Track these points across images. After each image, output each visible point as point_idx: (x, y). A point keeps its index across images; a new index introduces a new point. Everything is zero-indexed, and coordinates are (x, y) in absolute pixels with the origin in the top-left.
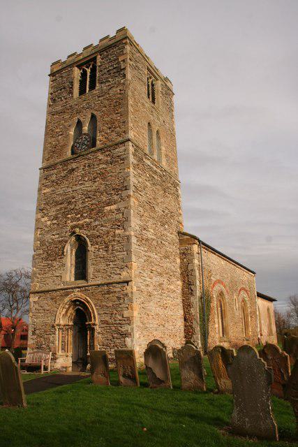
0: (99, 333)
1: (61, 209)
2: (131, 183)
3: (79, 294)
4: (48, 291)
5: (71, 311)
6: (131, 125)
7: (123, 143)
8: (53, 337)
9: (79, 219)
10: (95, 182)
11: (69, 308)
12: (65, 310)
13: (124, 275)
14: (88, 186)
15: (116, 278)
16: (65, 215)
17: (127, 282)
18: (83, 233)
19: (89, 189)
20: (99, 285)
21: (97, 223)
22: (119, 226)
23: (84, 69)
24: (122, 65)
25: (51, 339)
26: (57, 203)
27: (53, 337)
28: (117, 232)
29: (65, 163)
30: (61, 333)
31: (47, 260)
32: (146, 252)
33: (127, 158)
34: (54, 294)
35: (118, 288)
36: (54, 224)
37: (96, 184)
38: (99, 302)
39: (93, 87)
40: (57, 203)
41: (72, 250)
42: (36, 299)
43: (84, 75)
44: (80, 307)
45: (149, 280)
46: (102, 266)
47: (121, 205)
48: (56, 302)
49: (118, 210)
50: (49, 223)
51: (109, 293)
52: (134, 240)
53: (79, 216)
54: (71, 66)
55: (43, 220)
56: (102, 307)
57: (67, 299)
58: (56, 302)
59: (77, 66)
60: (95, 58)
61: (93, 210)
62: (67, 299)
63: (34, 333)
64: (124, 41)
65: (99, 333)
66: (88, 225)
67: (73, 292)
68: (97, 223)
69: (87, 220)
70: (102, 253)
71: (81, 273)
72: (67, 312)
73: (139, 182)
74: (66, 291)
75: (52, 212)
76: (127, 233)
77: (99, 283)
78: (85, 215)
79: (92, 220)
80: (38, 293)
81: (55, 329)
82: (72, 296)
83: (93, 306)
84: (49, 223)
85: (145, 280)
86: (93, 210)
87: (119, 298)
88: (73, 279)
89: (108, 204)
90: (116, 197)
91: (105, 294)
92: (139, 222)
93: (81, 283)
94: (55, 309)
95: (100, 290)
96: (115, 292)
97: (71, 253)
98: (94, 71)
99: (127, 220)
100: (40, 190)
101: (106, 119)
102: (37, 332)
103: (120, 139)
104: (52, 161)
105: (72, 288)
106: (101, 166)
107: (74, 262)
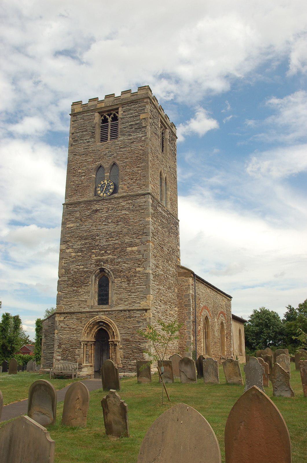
0: (121, 348)
1: (86, 244)
2: (151, 231)
3: (104, 317)
4: (74, 313)
5: (95, 330)
6: (150, 179)
7: (144, 195)
8: (79, 351)
9: (103, 255)
10: (118, 225)
11: (93, 327)
12: (89, 329)
13: (143, 304)
14: (111, 227)
15: (136, 306)
16: (91, 248)
17: (146, 310)
18: (107, 267)
19: (113, 230)
20: (121, 311)
21: (119, 260)
22: (139, 264)
23: (105, 117)
24: (143, 123)
25: (77, 352)
26: (81, 238)
27: (79, 351)
28: (138, 269)
29: (89, 203)
30: (85, 347)
31: (72, 286)
32: (158, 285)
33: (147, 209)
34: (80, 315)
35: (138, 314)
36: (78, 256)
37: (119, 227)
38: (121, 324)
39: (115, 135)
40: (81, 238)
41: (95, 280)
42: (62, 319)
43: (105, 121)
44: (103, 328)
45: (159, 307)
46: (124, 295)
47: (142, 248)
49: (139, 251)
50: (73, 254)
51: (130, 317)
52: (151, 277)
53: (103, 252)
54: (92, 111)
55: (68, 251)
56: (124, 328)
57: (91, 320)
59: (98, 112)
60: (118, 109)
61: (116, 249)
63: (59, 347)
64: (145, 101)
65: (121, 348)
66: (112, 261)
67: (97, 315)
68: (119, 260)
69: (110, 256)
70: (124, 285)
71: (103, 299)
72: (91, 330)
73: (155, 229)
74: (91, 314)
75: (78, 245)
76: (147, 271)
77: (121, 309)
78: (109, 252)
79: (116, 257)
80: (64, 313)
81: (81, 344)
82: (97, 318)
83: (116, 327)
84: (73, 254)
85: (157, 308)
86: (116, 249)
87: (138, 322)
88: (96, 304)
89: (131, 245)
90: (137, 241)
91: (127, 318)
92: (154, 262)
93: (104, 307)
94: (81, 328)
96: (136, 317)
97: (95, 282)
98: (115, 119)
99: (146, 260)
100: (64, 224)
101: (128, 170)
102: (63, 346)
103: (140, 192)
104: (75, 199)
105: (97, 312)
106: (124, 212)
107: (97, 290)
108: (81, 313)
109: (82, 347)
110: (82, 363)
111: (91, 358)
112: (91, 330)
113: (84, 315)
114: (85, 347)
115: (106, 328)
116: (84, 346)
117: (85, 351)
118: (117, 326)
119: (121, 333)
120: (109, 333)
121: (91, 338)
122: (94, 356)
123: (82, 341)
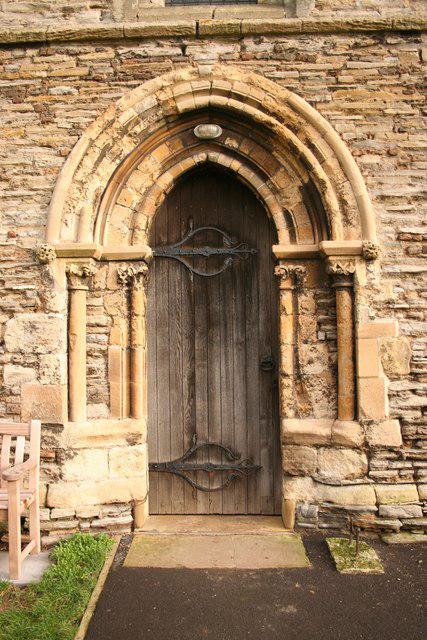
0: (389, 306)
5: (155, 176)
11: (141, 154)
12: (108, 167)
38: (384, 129)
44: (222, 159)
48: (46, 117)
57: (136, 102)
58: (46, 117)
62: (136, 102)
65: (389, 306)
67: (184, 58)
72: (119, 179)
82: (184, 87)
83: (346, 152)
94: (46, 157)
95: (388, 61)
108: (39, 43)
109: (59, 300)
110: (64, 420)
111: (131, 376)
112: (119, 179)
113: (62, 62)
114: (80, 299)
115: (245, 161)
116: (71, 291)
117: (80, 330)
118: (349, 143)
119: (383, 198)
120: (269, 198)
121: (125, 232)
122: (160, 356)
123: (62, 255)
